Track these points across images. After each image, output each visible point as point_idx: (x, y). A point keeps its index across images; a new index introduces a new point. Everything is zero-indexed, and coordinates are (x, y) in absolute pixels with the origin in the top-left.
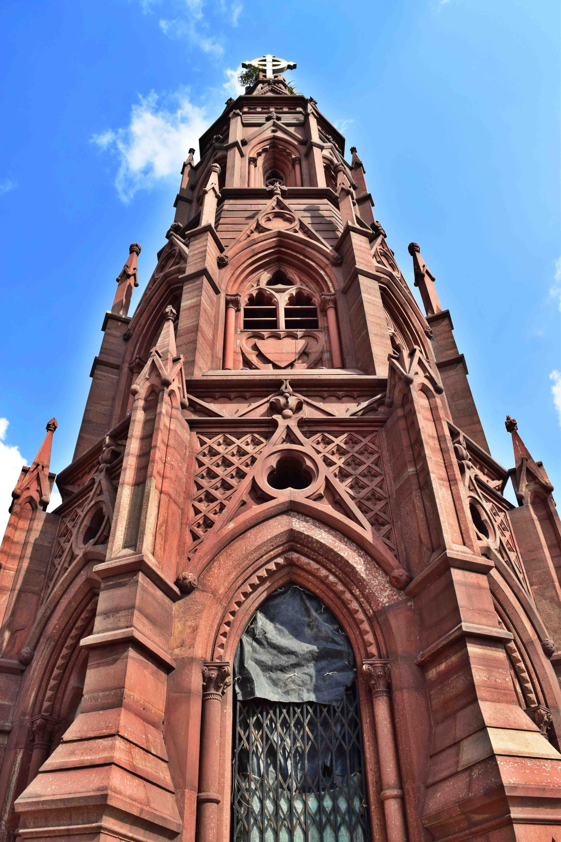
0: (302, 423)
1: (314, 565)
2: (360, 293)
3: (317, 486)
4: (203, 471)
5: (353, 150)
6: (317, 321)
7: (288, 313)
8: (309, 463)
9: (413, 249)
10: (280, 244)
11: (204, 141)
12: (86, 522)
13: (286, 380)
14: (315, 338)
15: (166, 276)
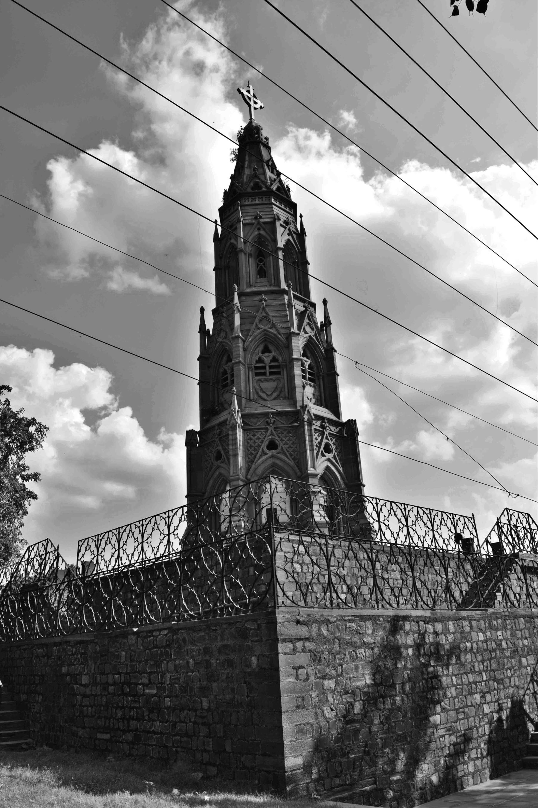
0: (275, 428)
1: (279, 471)
2: (294, 370)
3: (279, 449)
4: (249, 445)
5: (301, 216)
6: (280, 371)
7: (271, 367)
8: (277, 442)
9: (325, 302)
10: (265, 334)
11: (221, 210)
12: (215, 454)
13: (270, 412)
14: (280, 380)
15: (221, 342)
